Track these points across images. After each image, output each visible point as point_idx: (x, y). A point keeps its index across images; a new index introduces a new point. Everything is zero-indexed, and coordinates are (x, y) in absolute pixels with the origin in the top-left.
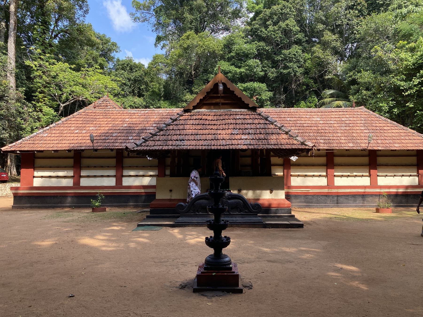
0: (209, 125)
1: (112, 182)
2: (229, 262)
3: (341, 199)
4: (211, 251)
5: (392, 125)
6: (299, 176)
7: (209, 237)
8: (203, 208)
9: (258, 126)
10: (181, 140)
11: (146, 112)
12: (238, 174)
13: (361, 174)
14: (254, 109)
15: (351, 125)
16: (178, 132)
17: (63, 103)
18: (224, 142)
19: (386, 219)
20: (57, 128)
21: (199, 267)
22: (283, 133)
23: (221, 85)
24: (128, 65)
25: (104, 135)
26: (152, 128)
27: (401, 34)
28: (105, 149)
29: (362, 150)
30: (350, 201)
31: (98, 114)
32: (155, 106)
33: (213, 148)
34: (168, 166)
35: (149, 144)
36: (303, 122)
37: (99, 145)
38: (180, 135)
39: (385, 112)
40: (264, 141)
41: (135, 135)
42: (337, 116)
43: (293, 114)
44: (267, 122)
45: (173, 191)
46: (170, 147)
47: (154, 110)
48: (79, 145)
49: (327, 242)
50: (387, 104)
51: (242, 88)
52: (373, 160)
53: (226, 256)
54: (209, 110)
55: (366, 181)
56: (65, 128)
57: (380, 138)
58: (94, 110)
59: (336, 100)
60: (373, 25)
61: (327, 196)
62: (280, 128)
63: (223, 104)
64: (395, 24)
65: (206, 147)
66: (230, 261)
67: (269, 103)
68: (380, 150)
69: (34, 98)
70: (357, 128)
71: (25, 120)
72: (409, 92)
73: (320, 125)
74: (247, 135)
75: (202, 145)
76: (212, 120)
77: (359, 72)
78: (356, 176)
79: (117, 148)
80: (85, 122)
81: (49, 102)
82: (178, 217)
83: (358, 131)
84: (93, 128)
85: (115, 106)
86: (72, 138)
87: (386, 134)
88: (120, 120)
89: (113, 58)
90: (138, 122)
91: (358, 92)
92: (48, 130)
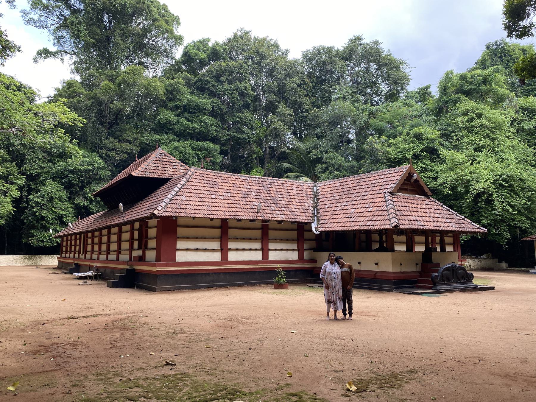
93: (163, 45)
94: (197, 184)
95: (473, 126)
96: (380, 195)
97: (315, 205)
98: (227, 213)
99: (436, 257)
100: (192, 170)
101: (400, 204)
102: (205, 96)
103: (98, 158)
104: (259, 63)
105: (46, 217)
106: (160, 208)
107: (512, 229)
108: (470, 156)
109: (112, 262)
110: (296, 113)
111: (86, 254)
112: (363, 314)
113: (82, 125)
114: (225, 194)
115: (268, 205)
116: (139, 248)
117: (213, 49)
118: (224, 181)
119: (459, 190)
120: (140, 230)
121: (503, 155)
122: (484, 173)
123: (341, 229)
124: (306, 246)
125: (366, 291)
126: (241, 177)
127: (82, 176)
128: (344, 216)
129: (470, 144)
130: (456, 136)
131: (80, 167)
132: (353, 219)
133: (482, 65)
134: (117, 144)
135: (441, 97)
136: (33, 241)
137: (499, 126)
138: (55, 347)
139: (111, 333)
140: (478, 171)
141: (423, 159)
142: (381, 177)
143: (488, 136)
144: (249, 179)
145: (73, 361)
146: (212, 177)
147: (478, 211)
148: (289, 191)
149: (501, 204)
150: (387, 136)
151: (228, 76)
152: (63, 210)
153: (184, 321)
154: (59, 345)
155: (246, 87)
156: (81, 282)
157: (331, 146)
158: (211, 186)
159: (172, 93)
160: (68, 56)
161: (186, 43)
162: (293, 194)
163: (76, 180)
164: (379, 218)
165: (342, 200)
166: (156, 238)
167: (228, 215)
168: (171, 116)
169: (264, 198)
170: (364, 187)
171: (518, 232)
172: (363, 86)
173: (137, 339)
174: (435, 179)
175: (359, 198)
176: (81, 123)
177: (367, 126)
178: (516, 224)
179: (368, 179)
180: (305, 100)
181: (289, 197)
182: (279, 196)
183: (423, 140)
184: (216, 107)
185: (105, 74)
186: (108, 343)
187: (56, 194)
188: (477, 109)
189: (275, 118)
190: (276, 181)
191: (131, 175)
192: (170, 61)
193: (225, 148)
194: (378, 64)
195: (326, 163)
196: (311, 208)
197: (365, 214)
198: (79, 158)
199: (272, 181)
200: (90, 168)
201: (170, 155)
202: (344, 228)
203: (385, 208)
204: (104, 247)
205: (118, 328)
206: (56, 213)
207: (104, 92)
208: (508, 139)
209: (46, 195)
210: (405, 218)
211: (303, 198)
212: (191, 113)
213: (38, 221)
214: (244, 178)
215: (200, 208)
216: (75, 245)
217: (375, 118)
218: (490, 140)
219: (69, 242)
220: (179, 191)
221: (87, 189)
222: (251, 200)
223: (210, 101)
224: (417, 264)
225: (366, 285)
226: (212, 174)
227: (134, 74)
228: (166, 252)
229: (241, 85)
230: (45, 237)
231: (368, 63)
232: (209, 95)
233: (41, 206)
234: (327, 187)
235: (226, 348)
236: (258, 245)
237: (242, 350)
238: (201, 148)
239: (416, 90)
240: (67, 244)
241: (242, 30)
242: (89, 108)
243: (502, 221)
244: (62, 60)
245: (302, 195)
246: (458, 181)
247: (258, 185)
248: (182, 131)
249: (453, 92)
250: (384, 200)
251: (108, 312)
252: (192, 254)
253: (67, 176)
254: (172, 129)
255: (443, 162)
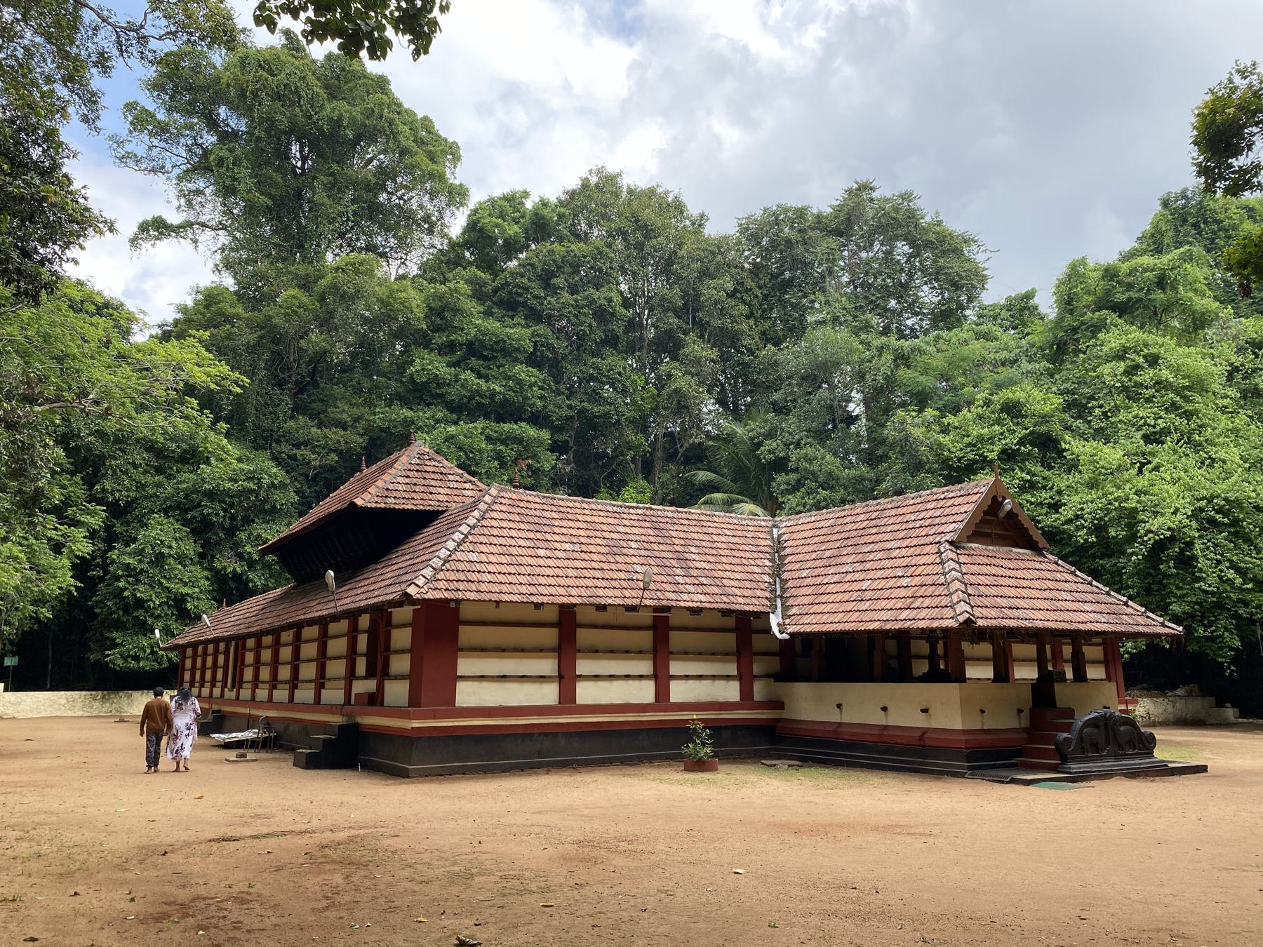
47: (651, 509)
93: (421, 207)
94: (504, 524)
95: (1140, 385)
96: (927, 549)
97: (777, 571)
98: (574, 592)
99: (1064, 694)
100: (493, 491)
101: (975, 569)
102: (517, 320)
103: (271, 463)
104: (640, 246)
105: (148, 601)
106: (421, 581)
107: (1244, 626)
108: (1136, 454)
109: (305, 707)
110: (725, 357)
111: (241, 687)
112: (898, 830)
113: (239, 390)
114: (567, 546)
115: (668, 571)
116: (370, 674)
117: (536, 214)
118: (561, 516)
119: (1113, 534)
120: (372, 632)
121: (1212, 451)
122: (1170, 494)
123: (839, 627)
124: (757, 669)
125: (902, 776)
126: (604, 508)
127: (232, 506)
128: (847, 597)
129: (1133, 425)
130: (1101, 406)
131: (228, 485)
132: (866, 605)
133: (1154, 243)
134: (314, 430)
135: (1060, 319)
136: (114, 658)
137: (1198, 385)
138: (201, 904)
139: (320, 873)
140: (1155, 490)
141: (1024, 460)
142: (930, 506)
143: (1174, 407)
144: (622, 510)
145: (248, 936)
146: (537, 506)
147: (1160, 582)
148: (716, 538)
149: (1214, 568)
150: (938, 409)
151: (570, 274)
152: (186, 585)
153: (484, 847)
154: (208, 902)
155: (610, 300)
156: (232, 754)
157: (809, 431)
158: (537, 528)
159: (442, 314)
160: (209, 233)
161: (472, 203)
162: (723, 546)
163: (217, 515)
164: (927, 602)
165: (839, 560)
166: (409, 651)
167: (575, 596)
168: (440, 367)
169: (657, 554)
170: (890, 528)
171: (1259, 632)
172: (879, 295)
173: (382, 887)
174: (1056, 507)
175: (880, 555)
176: (238, 386)
177: (891, 381)
178: (1252, 614)
179: (900, 511)
180: (744, 327)
181: (714, 552)
182: (693, 549)
183: (1023, 416)
184: (542, 345)
185: (290, 273)
186: (319, 896)
187: (170, 547)
188: (1146, 345)
189: (676, 369)
190: (684, 516)
191: (353, 504)
192: (437, 241)
193: (562, 437)
194: (912, 244)
195: (796, 470)
196: (766, 578)
197: (896, 593)
198: (229, 462)
199: (675, 515)
200: (251, 485)
201: (439, 458)
202: (847, 627)
203: (942, 580)
204: (285, 673)
205: (334, 862)
206: (170, 592)
207: (287, 314)
208: (1223, 413)
209: (148, 550)
210: (987, 601)
211: (748, 555)
212: (485, 358)
213: (127, 610)
214: (611, 509)
215: (511, 579)
216: (215, 667)
217: (909, 367)
218: (1180, 415)
219: (199, 660)
220: (463, 541)
221: (243, 536)
222: (628, 560)
223: (529, 331)
224: (1020, 711)
225: (901, 762)
226: (537, 500)
227: (357, 272)
228: (434, 684)
229: (599, 296)
230: (143, 649)
231: (891, 240)
232: (526, 319)
233: (136, 576)
234: (803, 529)
235: (587, 909)
236: (645, 667)
237: (625, 914)
238: (508, 438)
239: (1003, 302)
240: (194, 663)
241: (600, 171)
242: (252, 349)
243: (1220, 606)
244: (195, 241)
245: (745, 547)
246: (1109, 512)
247: (643, 524)
248: (465, 400)
249: (1087, 307)
250: (938, 561)
251: (307, 826)
252: (493, 688)
253: (199, 505)
254: (442, 396)
255: (1072, 467)
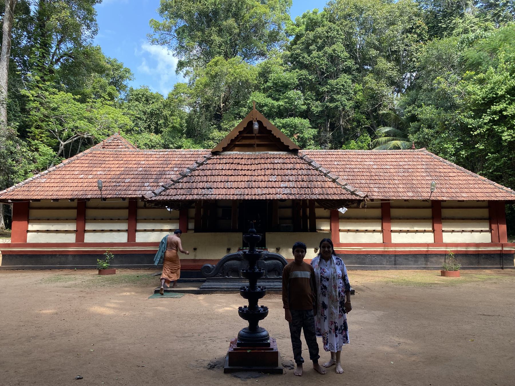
0: (241, 170)
1: (123, 238)
2: (267, 337)
3: (399, 260)
4: (246, 324)
5: (458, 171)
6: (349, 231)
7: (243, 307)
8: (235, 271)
9: (300, 172)
10: (208, 189)
11: (166, 153)
12: (277, 229)
13: (423, 229)
14: (295, 152)
15: (410, 170)
16: (205, 179)
17: (64, 141)
18: (259, 191)
19: (452, 284)
20: (58, 173)
21: (231, 343)
22: (330, 180)
23: (256, 123)
24: (143, 96)
25: (114, 180)
26: (173, 173)
27: (467, 63)
28: (116, 198)
29: (423, 200)
30: (410, 262)
31: (108, 156)
32: (175, 145)
33: (246, 197)
34: (192, 218)
35: (169, 192)
36: (353, 166)
37: (107, 193)
38: (206, 182)
39: (451, 154)
40: (307, 190)
41: (152, 180)
42: (393, 160)
43: (342, 156)
44: (311, 167)
45: (198, 250)
46: (195, 197)
47: (175, 151)
48: (84, 193)
49: (383, 312)
50: (454, 146)
51: (281, 125)
52: (437, 212)
53: (263, 330)
54: (241, 153)
55: (429, 238)
56: (68, 173)
57: (444, 186)
58: (103, 151)
59: (393, 140)
60: (435, 52)
61: (383, 255)
62: (325, 175)
63: (258, 145)
64: (460, 51)
65: (239, 197)
66: (268, 335)
67: (312, 142)
68: (445, 201)
69: (28, 134)
70: (418, 174)
71: (17, 162)
72: (478, 131)
73: (373, 170)
74: (287, 182)
75: (233, 195)
76: (245, 164)
77: (420, 106)
78: (417, 231)
79: (130, 196)
80: (91, 165)
81: (47, 139)
82: (204, 281)
83: (419, 178)
84: (101, 172)
85: (128, 145)
86: (76, 184)
87: (451, 182)
88: (134, 162)
89: (126, 86)
90: (155, 166)
91: (419, 130)
92: (47, 174)
